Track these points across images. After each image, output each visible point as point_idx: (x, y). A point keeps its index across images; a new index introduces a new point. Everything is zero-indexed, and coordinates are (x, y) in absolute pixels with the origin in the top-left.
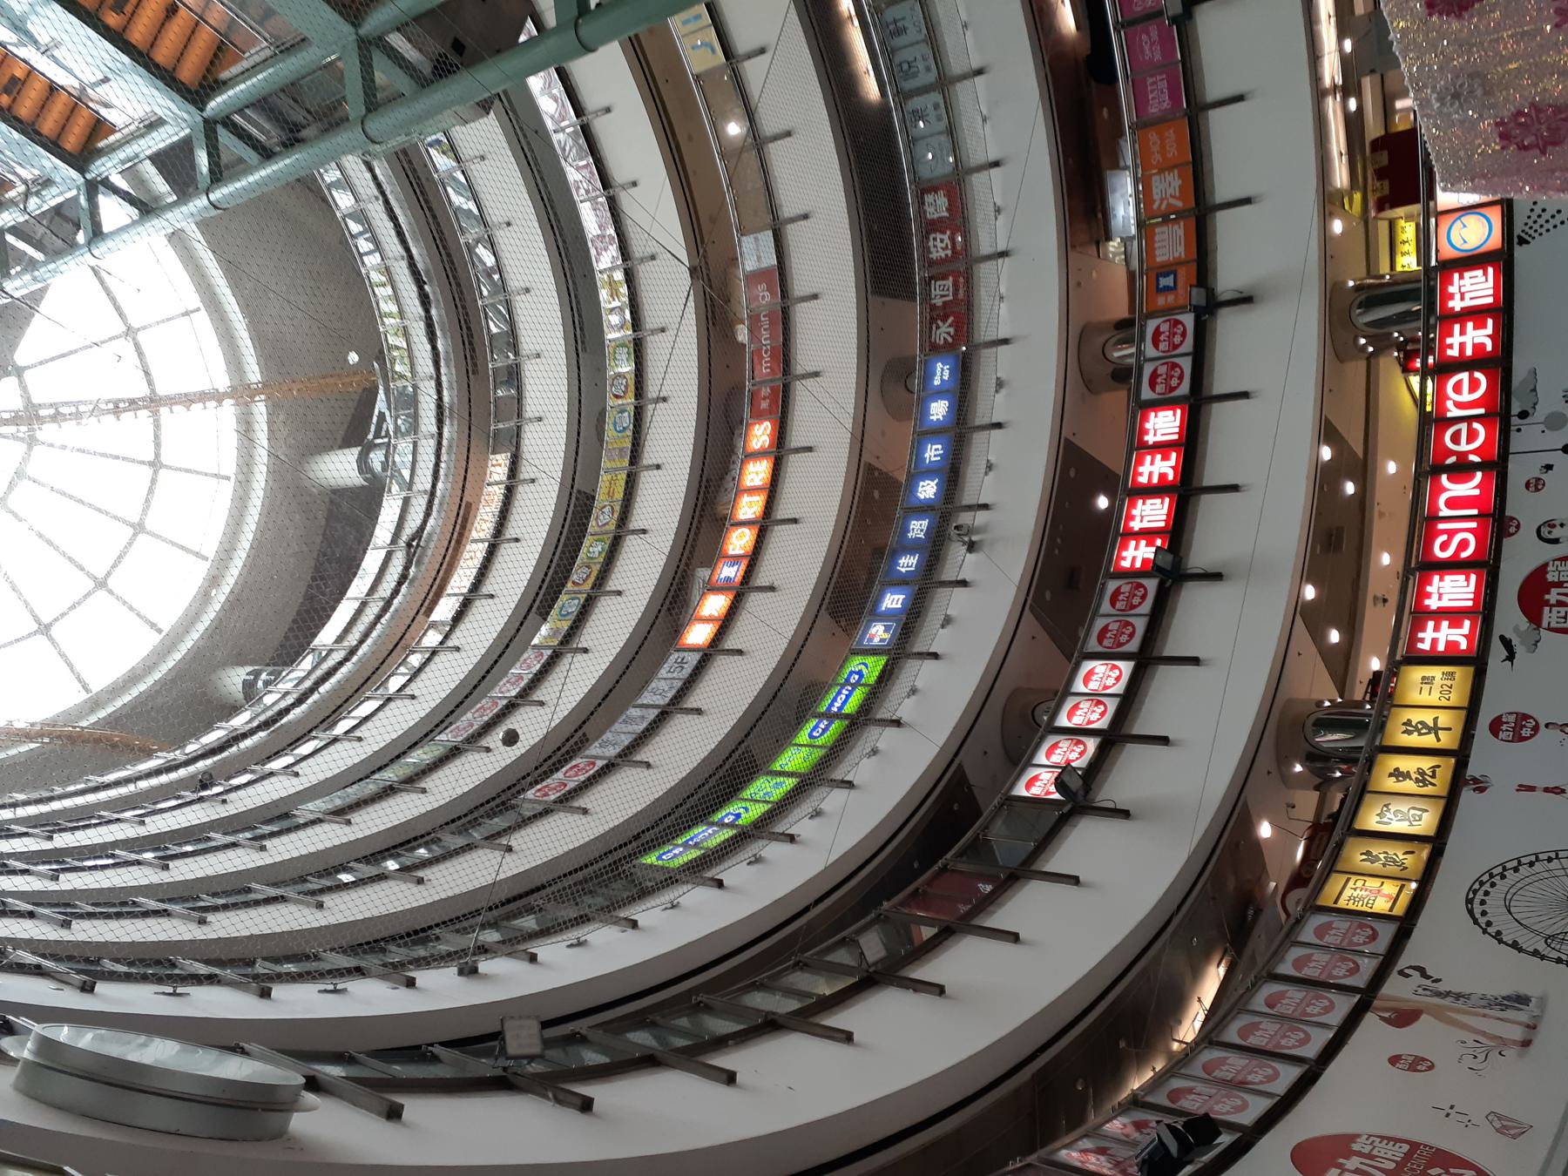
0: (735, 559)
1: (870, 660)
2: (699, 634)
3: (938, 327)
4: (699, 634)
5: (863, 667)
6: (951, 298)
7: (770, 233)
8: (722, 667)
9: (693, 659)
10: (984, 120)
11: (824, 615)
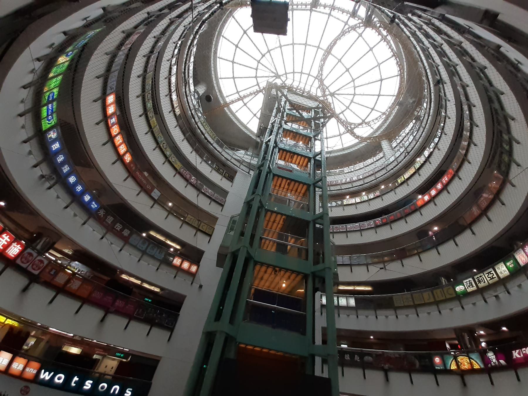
0: (113, 124)
1: (49, 126)
2: (111, 99)
3: (104, 212)
4: (111, 99)
5: (50, 122)
6: (107, 220)
7: (156, 199)
8: (98, 93)
9: (108, 92)
10: (130, 255)
11: (72, 122)
